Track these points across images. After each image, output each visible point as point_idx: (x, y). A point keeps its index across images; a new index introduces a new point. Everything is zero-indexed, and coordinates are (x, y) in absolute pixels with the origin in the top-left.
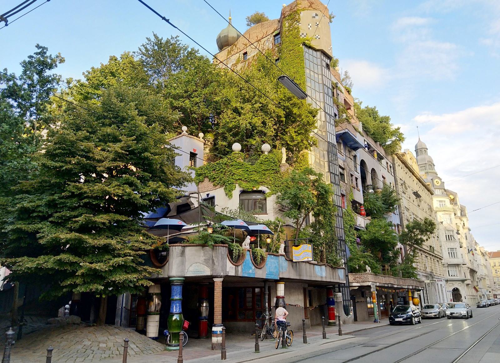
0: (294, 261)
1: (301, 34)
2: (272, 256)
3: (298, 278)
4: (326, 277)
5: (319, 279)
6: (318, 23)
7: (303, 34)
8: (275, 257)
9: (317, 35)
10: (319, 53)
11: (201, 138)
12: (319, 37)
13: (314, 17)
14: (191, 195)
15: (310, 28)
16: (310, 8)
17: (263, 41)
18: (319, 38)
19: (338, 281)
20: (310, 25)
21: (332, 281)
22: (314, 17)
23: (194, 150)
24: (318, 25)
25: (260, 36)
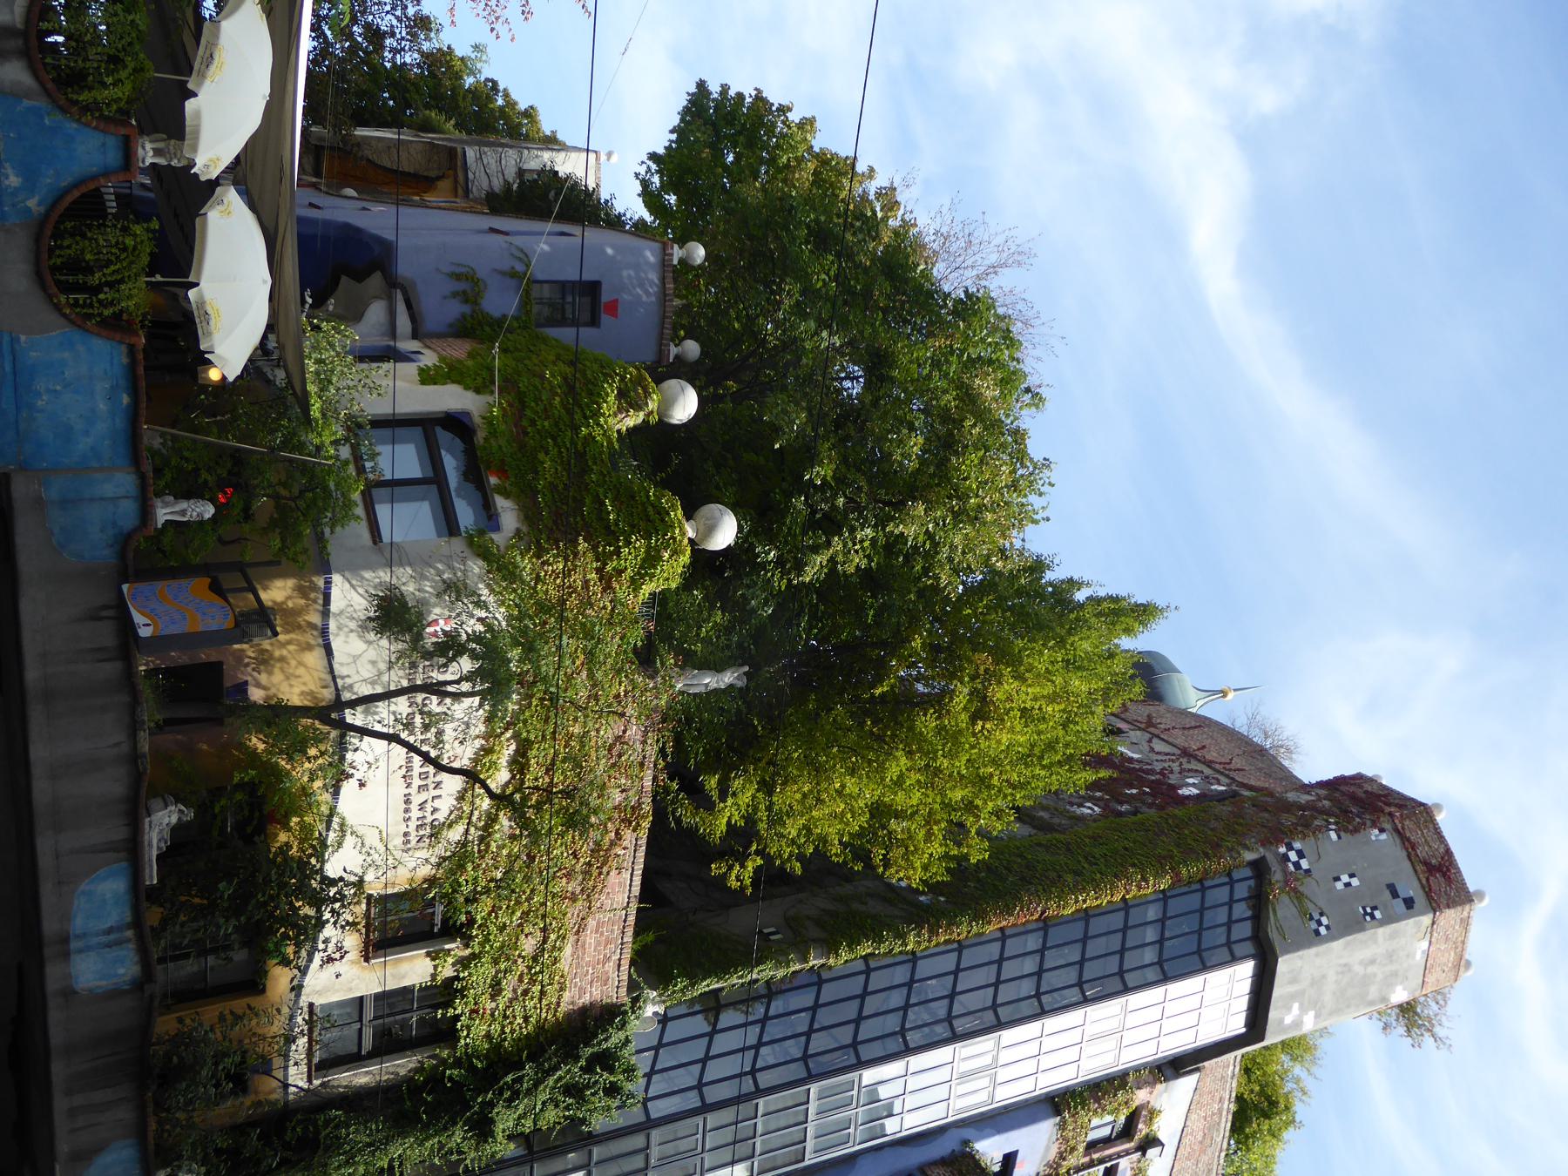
0: (125, 587)
1: (1297, 845)
2: (126, 399)
3: (32, 674)
4: (69, 993)
5: (49, 926)
6: (1377, 914)
7: (1301, 854)
8: (120, 423)
9: (1324, 920)
10: (1249, 947)
11: (674, 350)
12: (1323, 930)
13: (1395, 894)
14: (399, 296)
15: (1339, 885)
16: (1420, 868)
17: (1194, 765)
18: (1317, 933)
19: (63, 1147)
20: (1355, 882)
21: (59, 1070)
22: (1395, 894)
23: (613, 308)
24: (1373, 917)
25: (1212, 755)
